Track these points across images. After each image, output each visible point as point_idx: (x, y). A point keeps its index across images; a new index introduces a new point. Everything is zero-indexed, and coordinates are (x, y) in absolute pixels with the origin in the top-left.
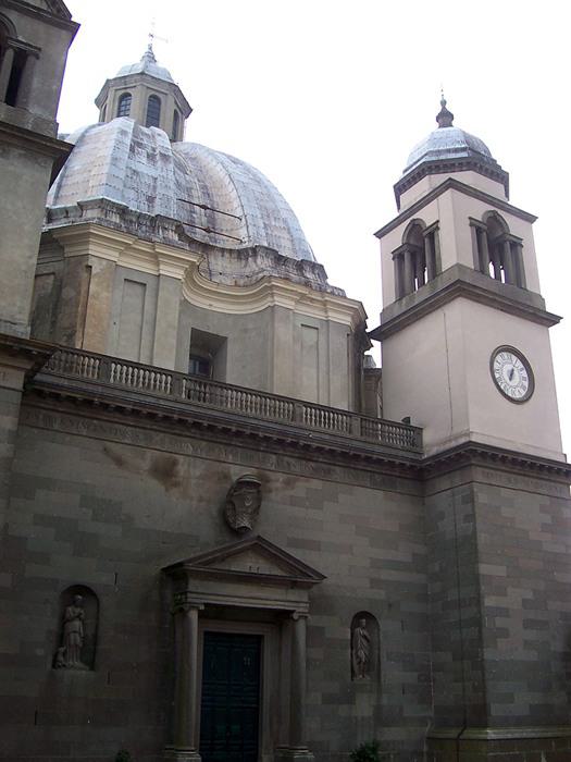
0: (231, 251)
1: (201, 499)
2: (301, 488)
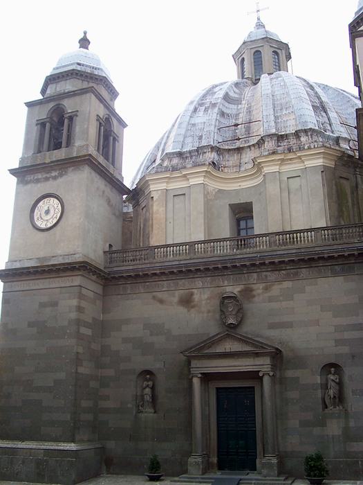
0: (253, 145)
1: (209, 312)
2: (276, 290)
